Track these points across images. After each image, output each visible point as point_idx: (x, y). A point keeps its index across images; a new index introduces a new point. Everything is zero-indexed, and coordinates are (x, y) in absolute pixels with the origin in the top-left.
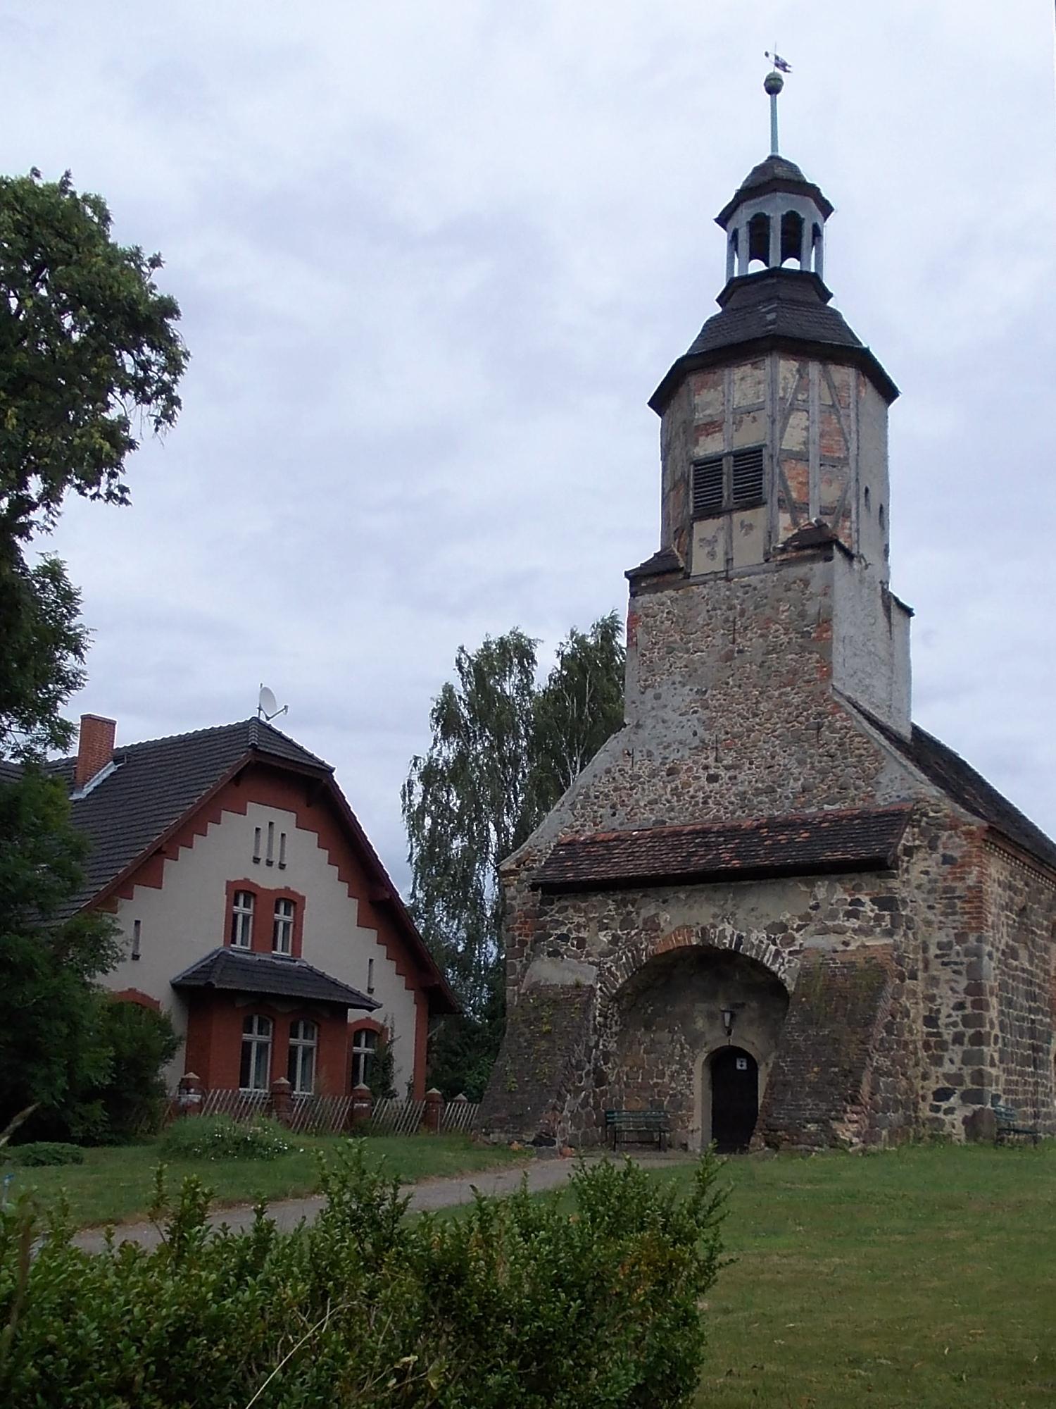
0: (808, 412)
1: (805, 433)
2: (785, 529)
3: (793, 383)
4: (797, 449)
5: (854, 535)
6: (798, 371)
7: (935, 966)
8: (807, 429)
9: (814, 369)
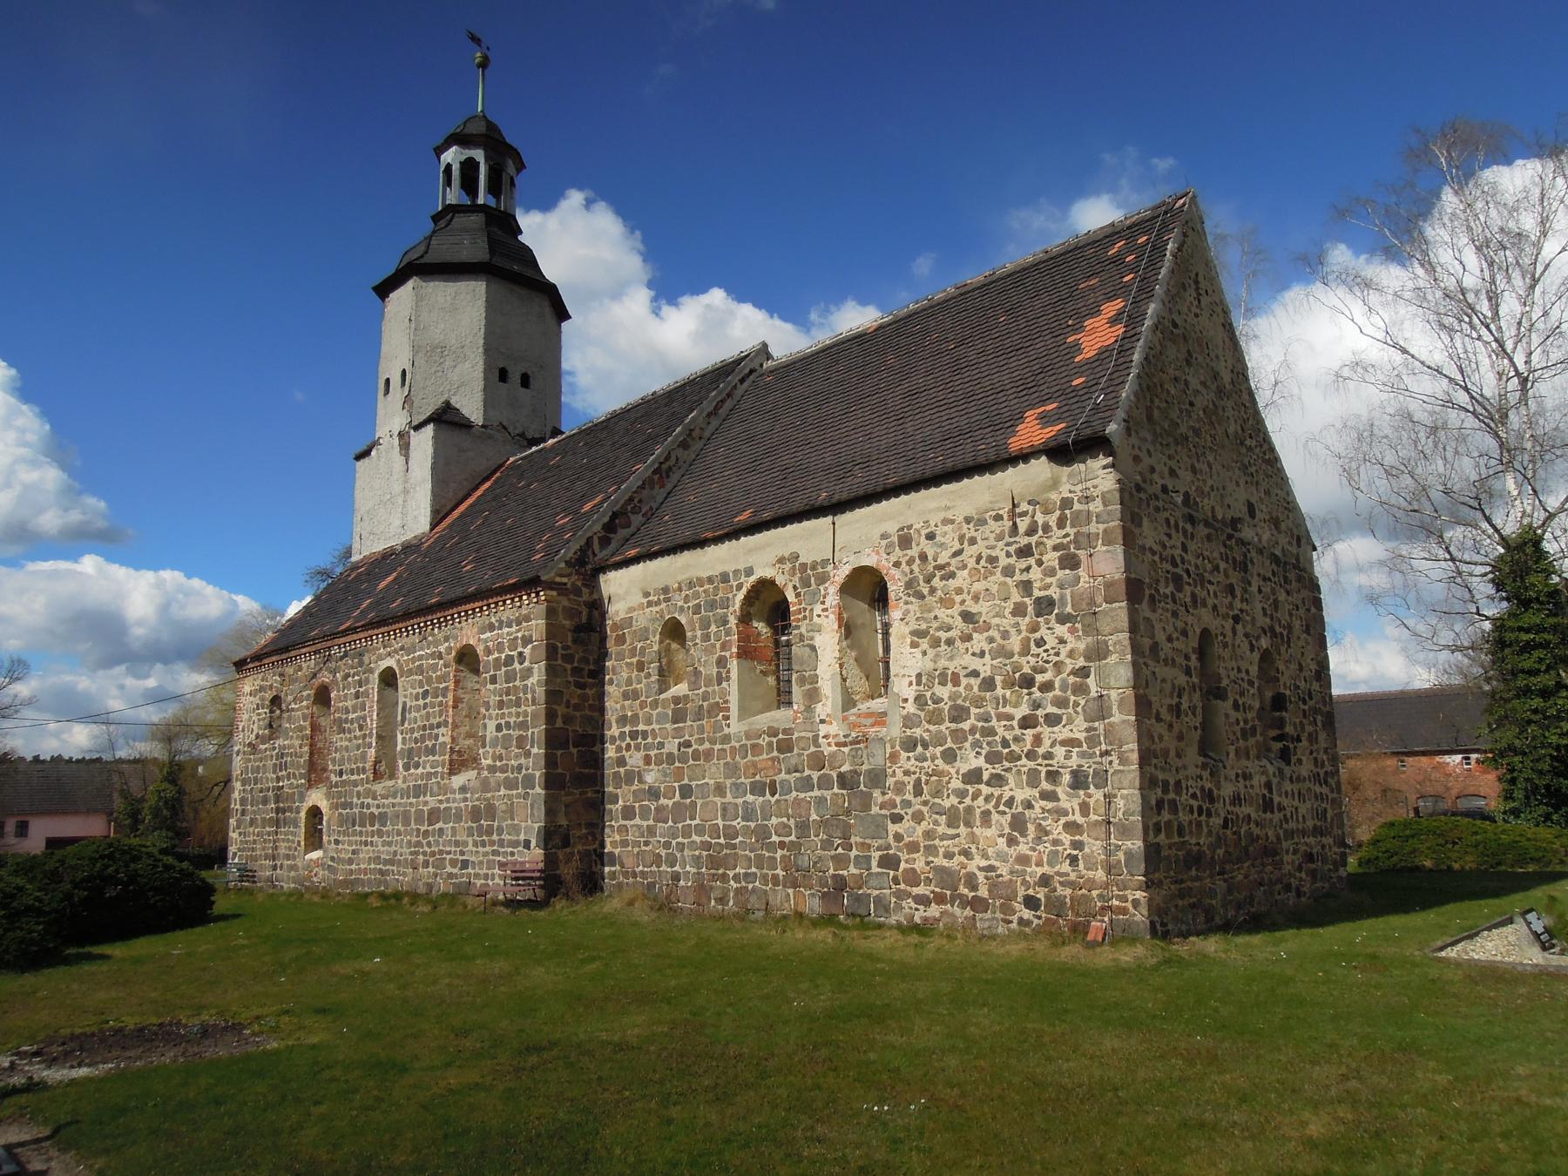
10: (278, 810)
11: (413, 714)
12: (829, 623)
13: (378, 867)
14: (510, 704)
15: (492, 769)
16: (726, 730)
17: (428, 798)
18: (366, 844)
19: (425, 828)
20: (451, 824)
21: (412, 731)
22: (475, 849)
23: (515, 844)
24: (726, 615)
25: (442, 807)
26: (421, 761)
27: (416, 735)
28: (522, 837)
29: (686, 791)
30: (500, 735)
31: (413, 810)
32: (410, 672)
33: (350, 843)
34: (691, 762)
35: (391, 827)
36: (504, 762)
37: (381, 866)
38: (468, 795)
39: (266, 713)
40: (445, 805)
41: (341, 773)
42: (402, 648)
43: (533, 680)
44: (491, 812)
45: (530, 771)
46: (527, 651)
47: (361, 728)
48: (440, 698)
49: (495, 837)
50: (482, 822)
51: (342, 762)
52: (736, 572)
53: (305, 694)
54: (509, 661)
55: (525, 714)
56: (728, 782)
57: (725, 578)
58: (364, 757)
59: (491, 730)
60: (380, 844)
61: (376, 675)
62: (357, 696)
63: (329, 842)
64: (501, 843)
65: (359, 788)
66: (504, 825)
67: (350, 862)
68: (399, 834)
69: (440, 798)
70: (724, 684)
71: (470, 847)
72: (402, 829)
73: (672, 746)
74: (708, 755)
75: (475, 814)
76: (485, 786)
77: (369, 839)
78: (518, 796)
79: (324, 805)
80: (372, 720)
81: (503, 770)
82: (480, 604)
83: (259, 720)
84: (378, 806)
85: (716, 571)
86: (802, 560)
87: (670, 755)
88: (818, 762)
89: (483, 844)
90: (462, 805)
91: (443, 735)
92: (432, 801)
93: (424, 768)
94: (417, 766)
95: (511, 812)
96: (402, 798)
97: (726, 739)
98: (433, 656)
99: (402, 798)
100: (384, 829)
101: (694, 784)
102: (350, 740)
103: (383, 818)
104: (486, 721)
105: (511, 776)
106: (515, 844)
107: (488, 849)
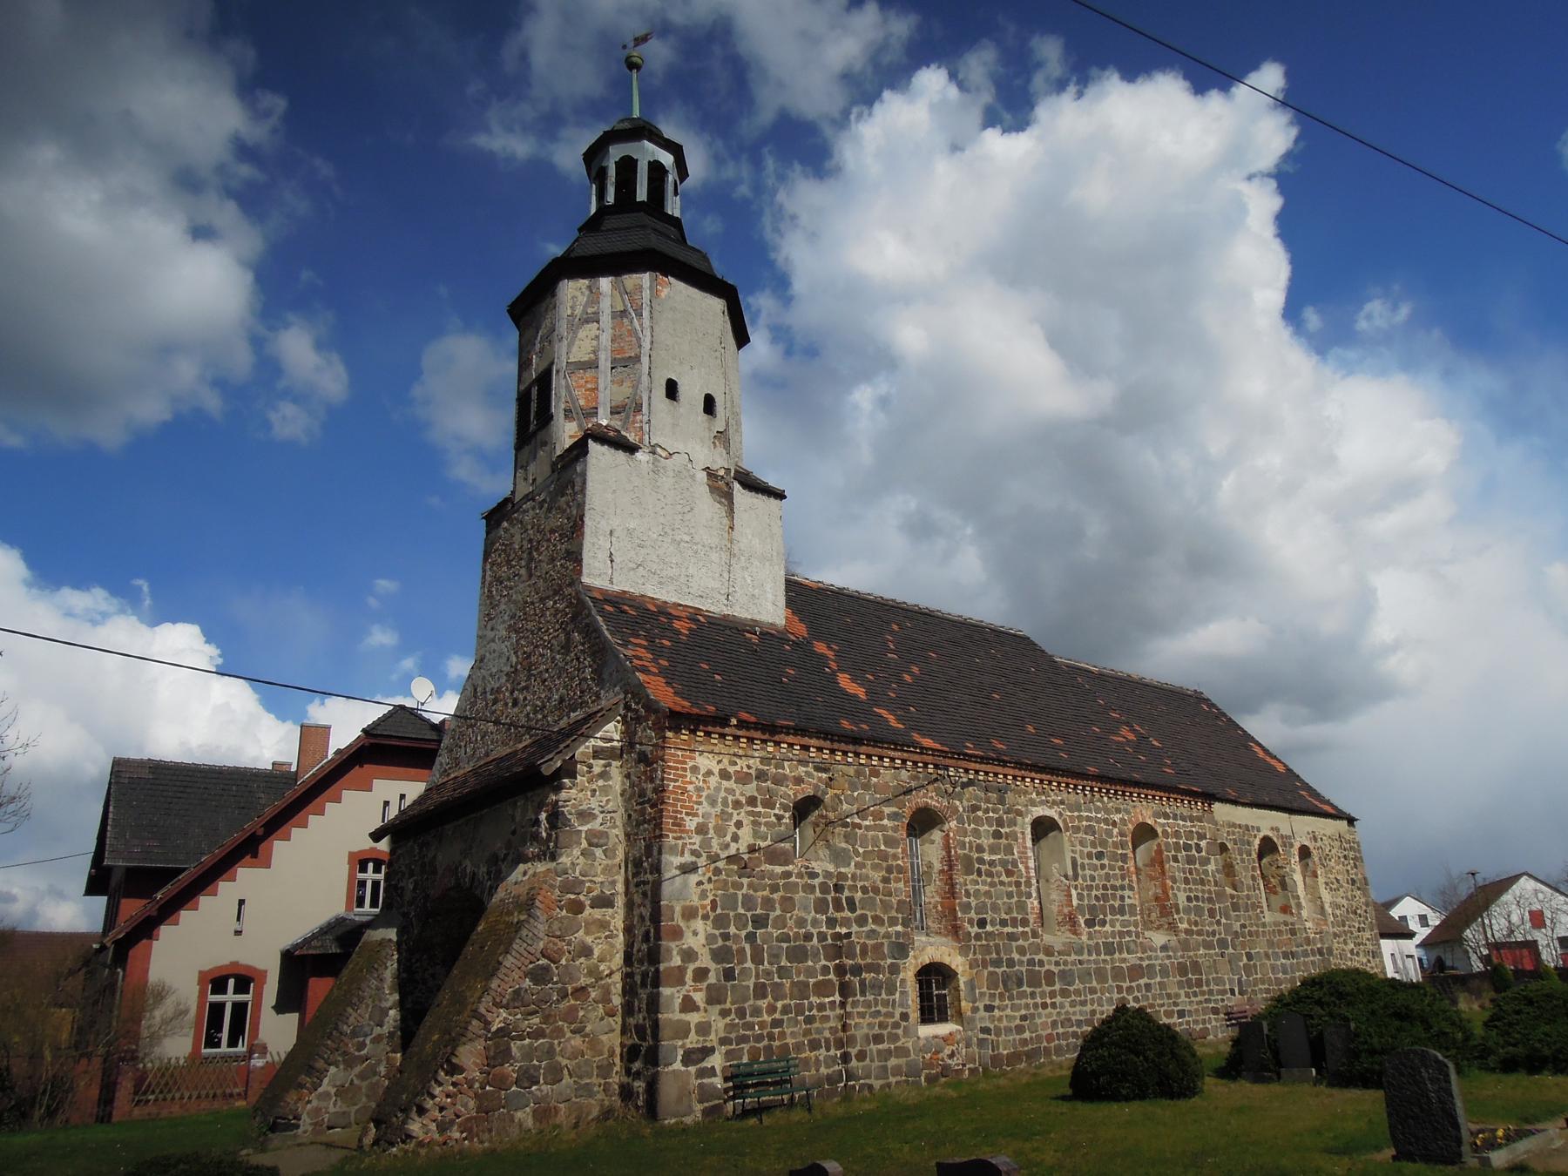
0: (598, 322)
1: (595, 343)
2: (571, 437)
3: (583, 299)
4: (586, 358)
5: (646, 427)
6: (589, 287)
7: (633, 889)
8: (597, 337)
9: (605, 283)
10: (840, 970)
12: (1298, 868)
13: (1071, 1030)
15: (1187, 932)
17: (1125, 955)
18: (1044, 1006)
19: (1128, 984)
21: (1090, 888)
22: (1187, 1000)
23: (1223, 992)
24: (1250, 850)
25: (1145, 964)
26: (1108, 919)
27: (1094, 892)
28: (1228, 987)
31: (1109, 967)
32: (1077, 829)
33: (1014, 1008)
35: (1081, 986)
36: (1200, 927)
37: (1075, 1029)
38: (1171, 953)
39: (779, 818)
41: (982, 923)
42: (1062, 802)
43: (1211, 867)
44: (1196, 967)
45: (1223, 936)
46: (1203, 843)
47: (1009, 873)
48: (1120, 864)
49: (1205, 988)
51: (981, 909)
53: (887, 810)
55: (1210, 892)
56: (1270, 951)
58: (1022, 907)
60: (1067, 1005)
61: (1029, 819)
62: (997, 835)
63: (975, 1010)
64: (1211, 992)
65: (1021, 942)
66: (1210, 977)
67: (1020, 1029)
68: (1093, 991)
70: (1257, 892)
71: (1183, 998)
72: (1098, 987)
75: (1182, 970)
76: (1185, 946)
77: (1049, 1001)
78: (1216, 954)
79: (957, 962)
80: (1027, 868)
81: (1199, 933)
82: (1162, 794)
83: (755, 823)
84: (1057, 963)
86: (1281, 832)
88: (1308, 941)
89: (1195, 995)
90: (1167, 962)
91: (1129, 897)
92: (1132, 959)
93: (1113, 926)
94: (1103, 923)
95: (1214, 967)
96: (1090, 954)
97: (1264, 925)
99: (1090, 954)
100: (1071, 988)
101: (1252, 951)
102: (992, 885)
103: (1066, 977)
106: (1223, 992)
107: (1200, 998)
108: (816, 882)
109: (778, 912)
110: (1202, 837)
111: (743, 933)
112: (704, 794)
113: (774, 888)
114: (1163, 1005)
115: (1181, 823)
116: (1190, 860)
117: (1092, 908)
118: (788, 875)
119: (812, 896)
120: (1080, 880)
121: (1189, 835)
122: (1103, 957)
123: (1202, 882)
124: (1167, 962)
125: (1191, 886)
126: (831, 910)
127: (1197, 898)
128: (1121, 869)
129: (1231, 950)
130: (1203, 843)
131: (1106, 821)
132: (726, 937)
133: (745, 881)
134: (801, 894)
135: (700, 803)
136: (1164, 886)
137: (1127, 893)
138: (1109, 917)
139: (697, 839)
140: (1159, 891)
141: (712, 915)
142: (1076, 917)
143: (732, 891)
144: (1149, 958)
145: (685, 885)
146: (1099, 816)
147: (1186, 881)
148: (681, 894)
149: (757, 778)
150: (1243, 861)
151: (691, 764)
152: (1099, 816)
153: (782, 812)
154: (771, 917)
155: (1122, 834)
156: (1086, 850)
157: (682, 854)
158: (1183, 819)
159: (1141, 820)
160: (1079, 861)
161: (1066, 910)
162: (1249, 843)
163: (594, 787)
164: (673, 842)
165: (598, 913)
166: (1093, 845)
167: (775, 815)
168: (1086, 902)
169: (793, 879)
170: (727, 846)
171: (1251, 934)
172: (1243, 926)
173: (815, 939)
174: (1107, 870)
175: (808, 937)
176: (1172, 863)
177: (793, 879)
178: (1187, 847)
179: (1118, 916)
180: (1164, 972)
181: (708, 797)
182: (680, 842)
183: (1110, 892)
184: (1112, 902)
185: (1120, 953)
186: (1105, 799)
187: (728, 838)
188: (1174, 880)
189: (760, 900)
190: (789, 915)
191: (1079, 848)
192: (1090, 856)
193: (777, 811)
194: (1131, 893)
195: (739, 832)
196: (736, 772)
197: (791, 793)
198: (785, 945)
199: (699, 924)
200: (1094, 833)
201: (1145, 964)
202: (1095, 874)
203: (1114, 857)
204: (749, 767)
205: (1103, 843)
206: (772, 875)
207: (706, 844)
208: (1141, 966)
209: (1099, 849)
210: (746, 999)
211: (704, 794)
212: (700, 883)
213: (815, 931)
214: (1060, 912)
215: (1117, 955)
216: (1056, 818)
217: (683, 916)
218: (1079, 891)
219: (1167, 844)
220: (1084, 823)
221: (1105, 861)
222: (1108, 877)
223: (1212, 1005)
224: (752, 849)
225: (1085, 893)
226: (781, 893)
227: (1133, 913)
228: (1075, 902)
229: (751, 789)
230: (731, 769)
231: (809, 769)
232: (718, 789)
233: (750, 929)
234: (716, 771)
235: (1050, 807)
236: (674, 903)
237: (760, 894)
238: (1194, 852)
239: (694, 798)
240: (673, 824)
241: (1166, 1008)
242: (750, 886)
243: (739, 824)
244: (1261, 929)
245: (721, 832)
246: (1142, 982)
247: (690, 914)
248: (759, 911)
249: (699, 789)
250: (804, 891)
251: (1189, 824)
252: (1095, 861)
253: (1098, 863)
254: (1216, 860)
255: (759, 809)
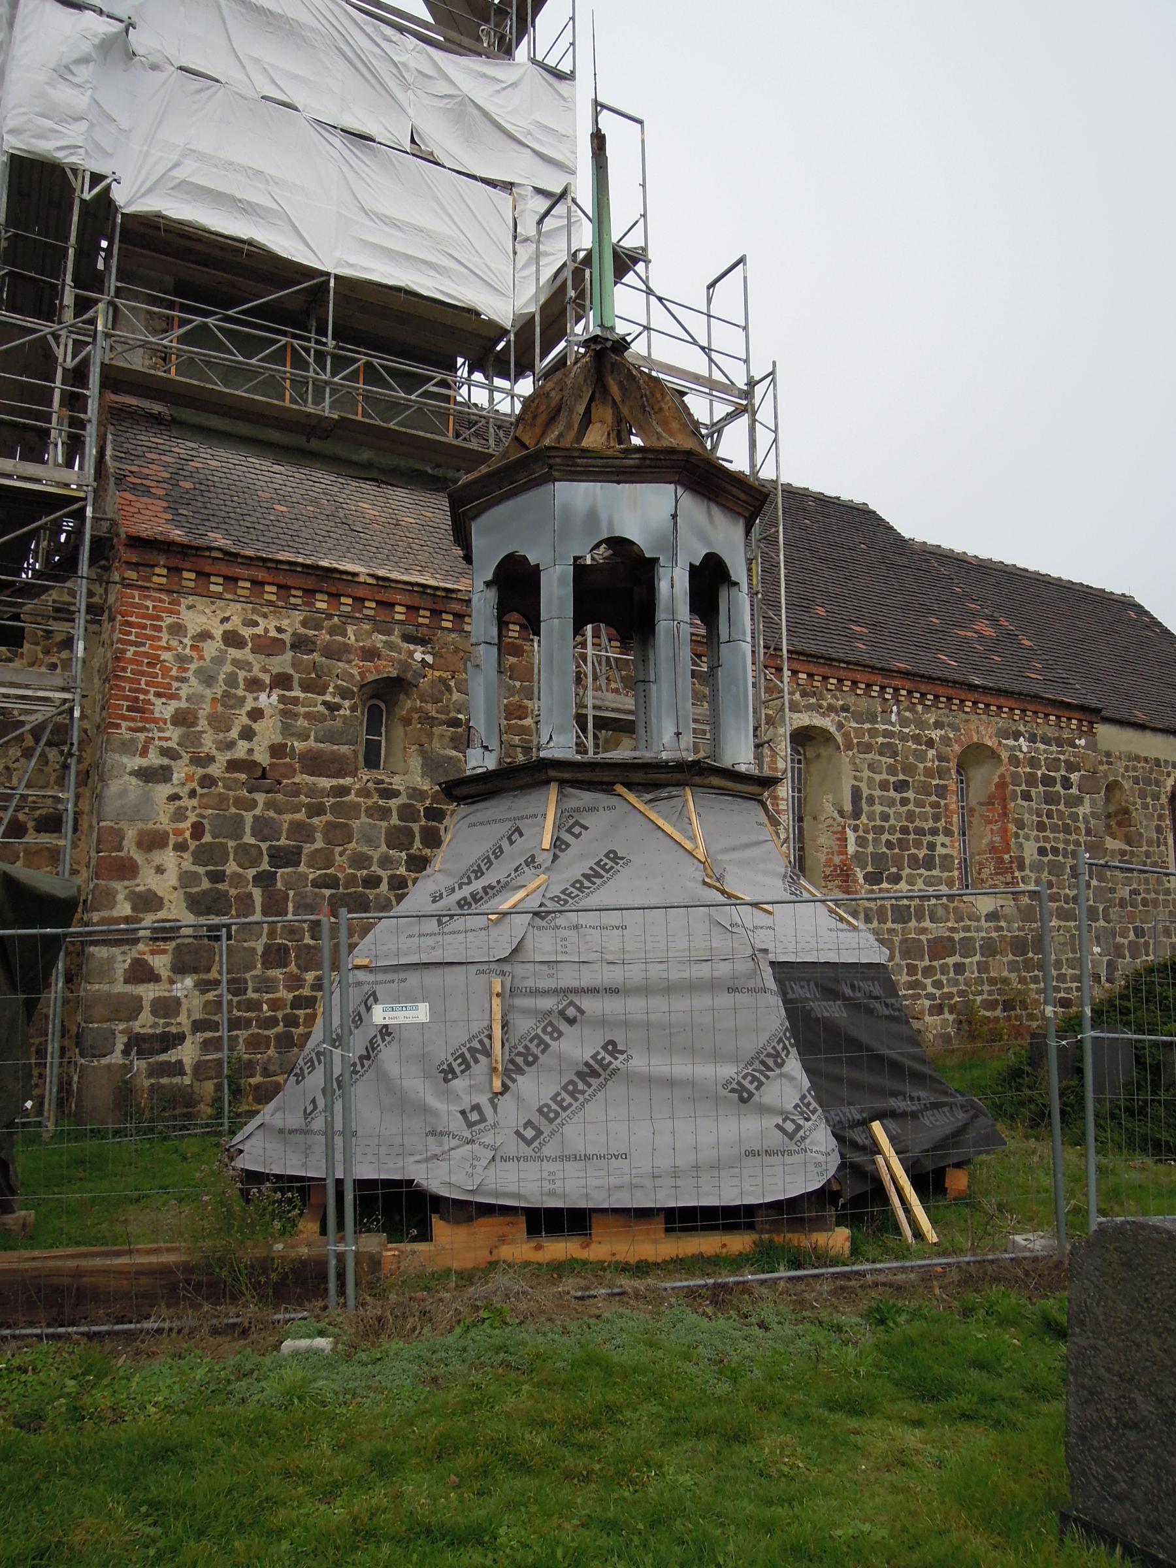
11: (878, 808)
14: (1055, 829)
16: (1168, 885)
17: (927, 924)
19: (927, 963)
20: (977, 958)
21: (879, 830)
25: (956, 937)
27: (885, 837)
29: (1139, 932)
30: (1045, 859)
32: (868, 748)
34: (1141, 908)
36: (1055, 890)
38: (1003, 924)
39: (332, 708)
40: (962, 934)
42: (845, 709)
43: (1084, 810)
46: (1074, 777)
48: (934, 798)
50: (1030, 955)
52: (1166, 762)
54: (1048, 781)
55: (1077, 843)
57: (1157, 762)
59: (1030, 851)
64: (1062, 978)
66: (1064, 958)
69: (950, 924)
70: (1162, 848)
73: (1124, 892)
74: (1155, 902)
81: (1054, 898)
85: (1152, 754)
87: (1122, 899)
90: (994, 935)
91: (943, 845)
92: (937, 930)
94: (896, 879)
98: (917, 739)
104: (1021, 840)
105: (1066, 906)
108: (393, 803)
109: (319, 844)
110: (1072, 767)
111: (251, 872)
112: (193, 667)
113: (316, 810)
114: (981, 993)
115: (1042, 747)
116: (1050, 799)
117: (878, 858)
118: (343, 791)
119: (384, 824)
120: (864, 819)
121: (1054, 764)
122: (889, 925)
123: (1067, 829)
124: (994, 935)
125: (1048, 833)
126: (417, 844)
127: (1055, 851)
128: (935, 805)
129: (1102, 923)
130: (1074, 777)
131: (917, 739)
132: (216, 877)
133: (261, 798)
134: (364, 819)
135: (184, 680)
136: (1004, 831)
137: (940, 839)
138: (904, 873)
139: (174, 734)
140: (997, 839)
141: (193, 845)
142: (849, 869)
143: (233, 810)
144: (967, 929)
145: (147, 799)
146: (906, 730)
147: (1041, 827)
148: (137, 813)
149: (293, 647)
150: (1145, 806)
151: (169, 621)
152: (906, 730)
153: (337, 700)
154: (305, 851)
155: (941, 758)
156: (878, 778)
157: (144, 753)
158: (1046, 741)
159: (975, 740)
160: (866, 792)
161: (837, 860)
162: (1158, 783)
163: (54, 660)
164: (128, 735)
165: (45, 839)
166: (892, 770)
167: (324, 703)
168: (870, 849)
169: (352, 797)
170: (231, 745)
171: (1145, 903)
172: (1134, 892)
173: (384, 886)
174: (911, 807)
175: (372, 882)
176: (1019, 801)
177: (352, 797)
178: (1048, 781)
179: (922, 871)
180: (990, 948)
181: (199, 672)
182: (142, 736)
183: (912, 836)
184: (913, 851)
185: (919, 921)
186: (919, 708)
187: (234, 734)
188: (1020, 825)
189: (286, 826)
190: (339, 849)
191: (866, 773)
192: (884, 786)
193: (328, 698)
194: (947, 840)
195: (255, 726)
196: (255, 637)
197: (355, 672)
198: (327, 892)
199: (169, 858)
200: (894, 754)
201: (956, 937)
202: (891, 811)
203: (925, 789)
204: (279, 630)
205: (909, 769)
206: (312, 791)
207: (191, 740)
208: (951, 939)
209: (901, 777)
210: (250, 967)
211: (193, 667)
212: (174, 797)
213: (384, 874)
214: (829, 862)
215: (913, 924)
216: (832, 729)
217: (139, 844)
218: (861, 833)
219: (1015, 776)
220: (880, 740)
221: (910, 795)
222: (910, 816)
223: (1062, 995)
224: (277, 751)
225: (870, 837)
226: (329, 817)
227: (944, 868)
228: (851, 848)
229: (283, 662)
230: (246, 632)
231: (393, 638)
232: (219, 660)
233: (265, 866)
234: (218, 633)
235: (823, 715)
236: (124, 825)
237: (287, 817)
238: (1058, 788)
239: (174, 673)
240: (129, 709)
241: (985, 997)
242: (269, 805)
243: (256, 714)
244: (1161, 897)
245: (220, 723)
246: (950, 961)
247: (153, 842)
248: (283, 842)
249: (182, 660)
250: (370, 816)
251: (1054, 748)
252: (892, 793)
253: (897, 796)
254: (1093, 801)
255: (297, 693)
